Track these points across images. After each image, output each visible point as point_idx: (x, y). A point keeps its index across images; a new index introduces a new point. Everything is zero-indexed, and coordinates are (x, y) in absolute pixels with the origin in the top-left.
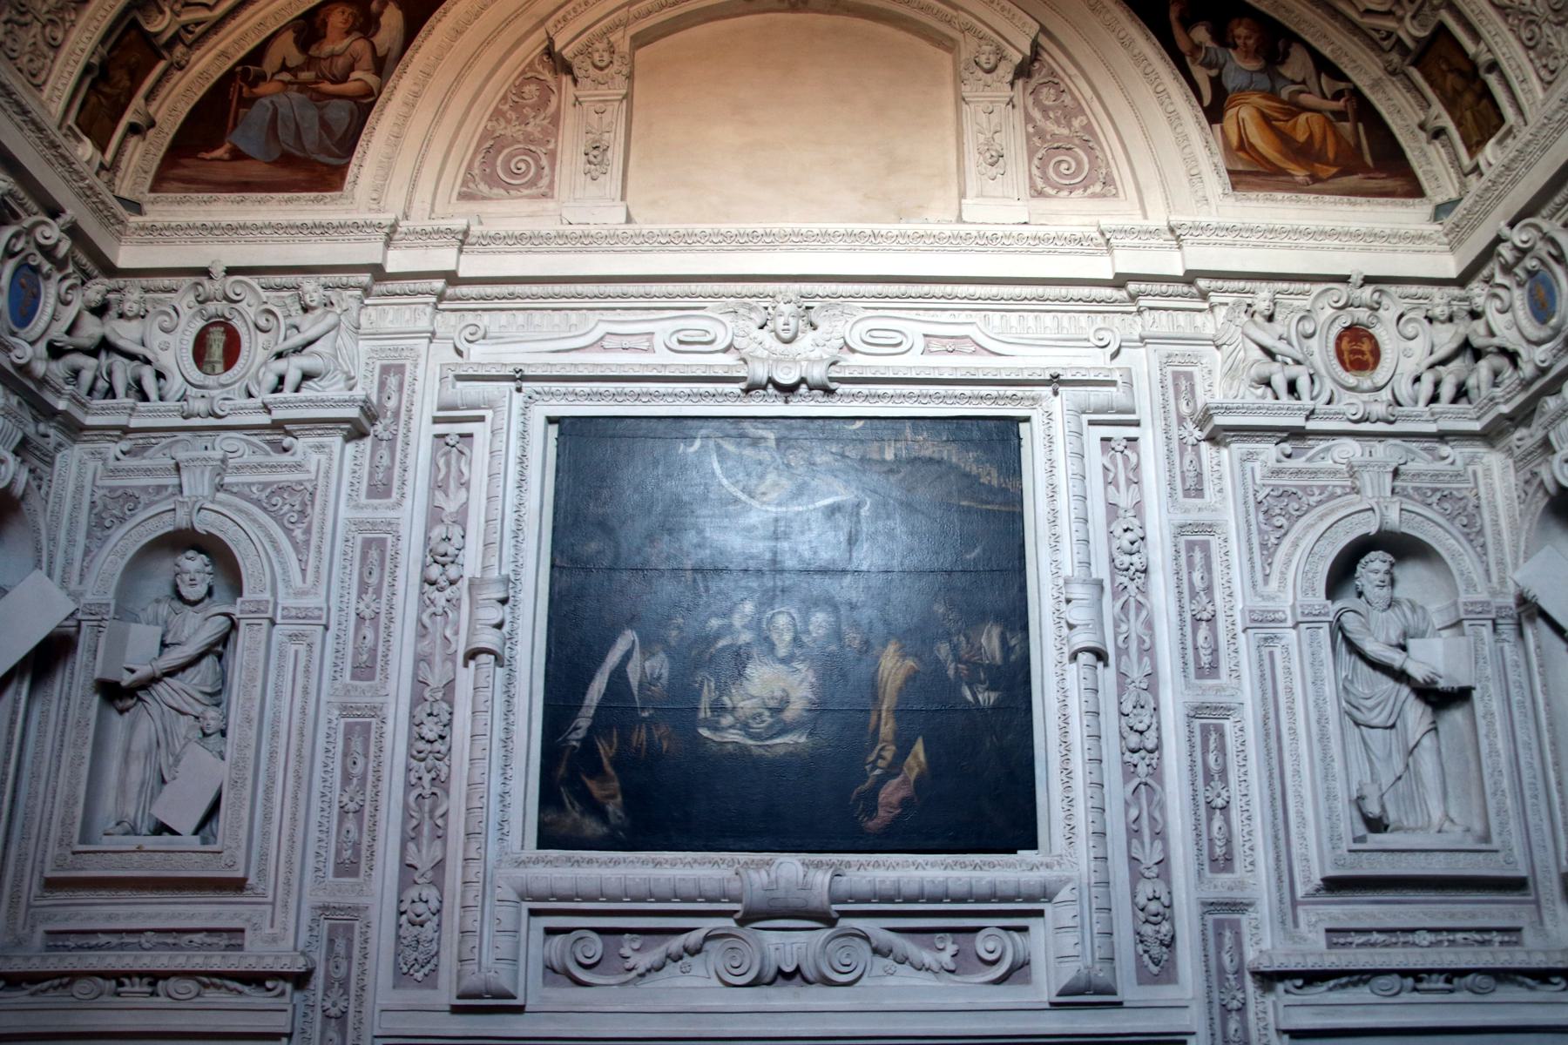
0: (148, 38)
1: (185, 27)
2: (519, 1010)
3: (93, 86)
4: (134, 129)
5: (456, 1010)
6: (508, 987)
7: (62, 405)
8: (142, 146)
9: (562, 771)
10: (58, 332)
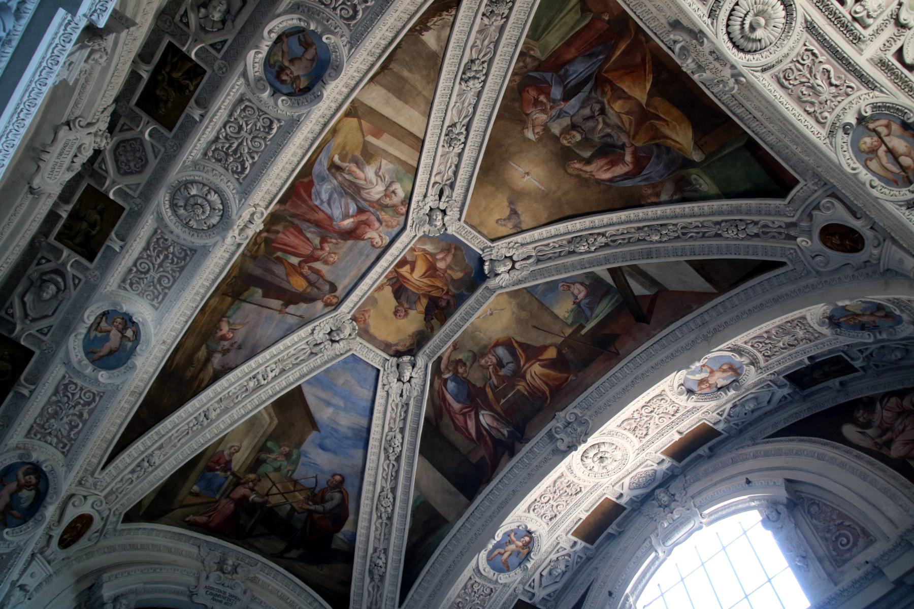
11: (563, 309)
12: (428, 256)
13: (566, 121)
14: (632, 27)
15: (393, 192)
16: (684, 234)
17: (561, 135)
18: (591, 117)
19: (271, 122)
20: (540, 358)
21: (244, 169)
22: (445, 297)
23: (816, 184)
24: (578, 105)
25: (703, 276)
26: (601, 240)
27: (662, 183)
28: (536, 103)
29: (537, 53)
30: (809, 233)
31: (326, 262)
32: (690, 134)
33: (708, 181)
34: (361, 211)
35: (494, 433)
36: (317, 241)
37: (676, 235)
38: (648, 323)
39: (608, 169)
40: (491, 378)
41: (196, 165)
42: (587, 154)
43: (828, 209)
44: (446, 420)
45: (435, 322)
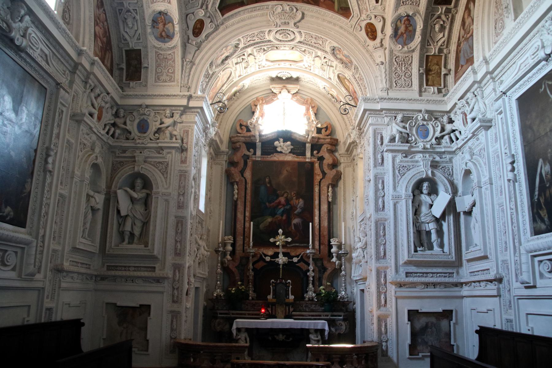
0: (434, 55)
1: (441, 46)
2: (534, 287)
3: (427, 75)
4: (446, 75)
5: (527, 287)
6: (528, 281)
7: (443, 150)
8: (451, 76)
9: (535, 210)
10: (438, 134)
14: (312, 2)
23: (220, 22)
30: (204, 16)
43: (211, 26)
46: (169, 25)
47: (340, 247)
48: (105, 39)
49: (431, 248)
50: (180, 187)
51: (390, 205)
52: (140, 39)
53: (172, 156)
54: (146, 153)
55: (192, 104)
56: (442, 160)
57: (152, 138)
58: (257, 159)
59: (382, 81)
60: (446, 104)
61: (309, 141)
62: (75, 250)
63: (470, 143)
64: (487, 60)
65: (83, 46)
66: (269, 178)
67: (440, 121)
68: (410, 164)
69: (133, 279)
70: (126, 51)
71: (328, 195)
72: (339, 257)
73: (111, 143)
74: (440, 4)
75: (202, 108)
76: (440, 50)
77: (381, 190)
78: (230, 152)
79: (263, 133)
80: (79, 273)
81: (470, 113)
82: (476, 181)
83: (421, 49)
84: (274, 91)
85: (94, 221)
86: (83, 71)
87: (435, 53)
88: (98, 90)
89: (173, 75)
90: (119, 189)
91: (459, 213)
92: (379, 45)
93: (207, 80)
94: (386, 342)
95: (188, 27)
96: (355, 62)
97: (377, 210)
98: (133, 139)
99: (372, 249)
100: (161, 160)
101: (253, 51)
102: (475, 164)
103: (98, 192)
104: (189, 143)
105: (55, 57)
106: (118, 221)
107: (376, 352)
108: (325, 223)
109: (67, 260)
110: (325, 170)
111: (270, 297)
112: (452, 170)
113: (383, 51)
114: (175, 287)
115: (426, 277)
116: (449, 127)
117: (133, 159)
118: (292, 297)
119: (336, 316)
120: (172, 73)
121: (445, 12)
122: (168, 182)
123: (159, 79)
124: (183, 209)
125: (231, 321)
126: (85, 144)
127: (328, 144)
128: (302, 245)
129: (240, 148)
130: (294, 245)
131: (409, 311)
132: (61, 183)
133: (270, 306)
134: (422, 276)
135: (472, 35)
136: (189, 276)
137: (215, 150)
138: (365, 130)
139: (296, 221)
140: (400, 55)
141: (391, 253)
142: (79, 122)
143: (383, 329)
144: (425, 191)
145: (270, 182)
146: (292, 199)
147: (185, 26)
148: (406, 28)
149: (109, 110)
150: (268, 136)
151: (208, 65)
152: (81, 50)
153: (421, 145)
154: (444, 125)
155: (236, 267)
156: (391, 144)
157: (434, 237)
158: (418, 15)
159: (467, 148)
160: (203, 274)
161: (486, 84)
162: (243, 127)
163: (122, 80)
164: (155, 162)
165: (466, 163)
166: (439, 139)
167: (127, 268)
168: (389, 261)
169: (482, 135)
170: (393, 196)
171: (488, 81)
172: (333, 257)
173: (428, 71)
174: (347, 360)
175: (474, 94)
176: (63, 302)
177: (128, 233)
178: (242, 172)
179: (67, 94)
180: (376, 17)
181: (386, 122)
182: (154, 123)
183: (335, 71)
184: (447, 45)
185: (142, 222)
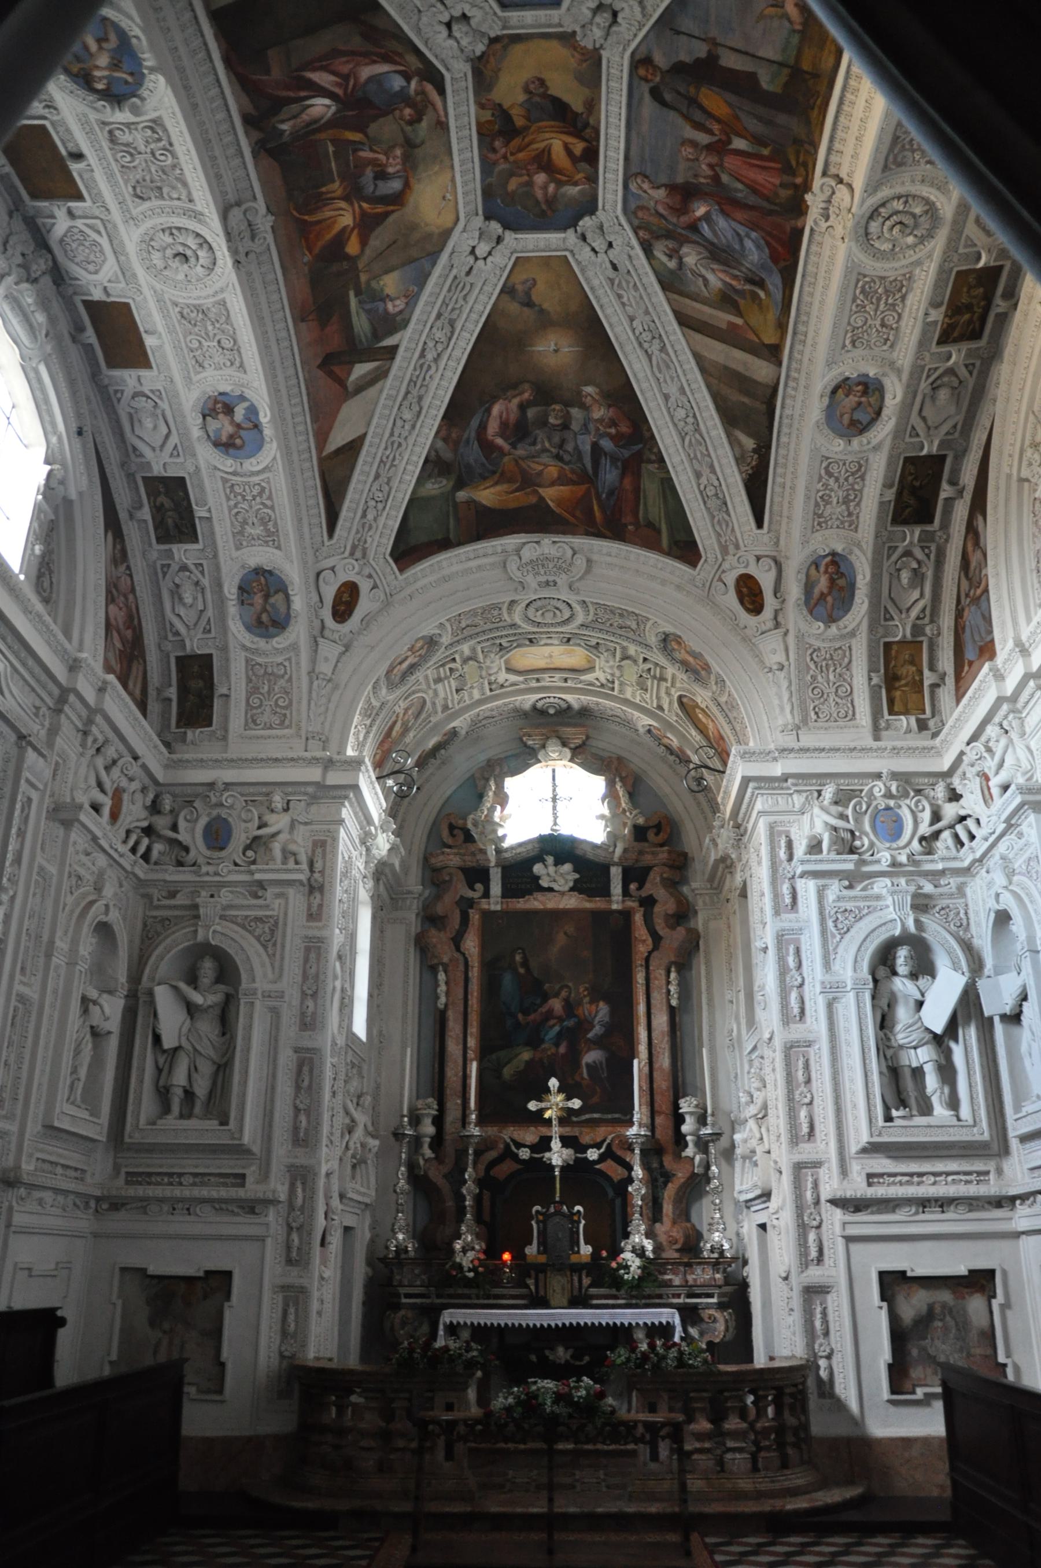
1: (918, 618)
4: (934, 686)
7: (940, 866)
10: (925, 829)
11: (390, 283)
12: (564, 178)
13: (575, 426)
14: (608, 533)
15: (670, 257)
16: (393, 443)
17: (568, 412)
18: (561, 446)
19: (854, 346)
20: (356, 232)
21: (863, 291)
22: (504, 150)
24: (581, 447)
25: (344, 446)
26: (430, 356)
27: (455, 451)
28: (613, 423)
29: (652, 467)
31: (694, 144)
32: (485, 502)
33: (434, 492)
34: (694, 227)
35: (294, 108)
36: (725, 178)
37: (396, 434)
38: (319, 367)
39: (501, 417)
40: (372, 150)
41: (918, 263)
42: (531, 413)
44: (357, 42)
45: (487, 115)
46: (277, 597)
47: (702, 1120)
48: (129, 634)
49: (926, 1109)
50: (305, 976)
51: (816, 1006)
52: (209, 631)
53: (287, 903)
54: (225, 896)
55: (334, 778)
56: (940, 890)
57: (238, 861)
58: (493, 908)
59: (782, 709)
60: (939, 754)
61: (616, 859)
62: (51, 1130)
63: (1002, 847)
64: (1023, 645)
65: (80, 650)
66: (524, 953)
67: (927, 798)
68: (861, 904)
69: (189, 1206)
70: (178, 658)
71: (669, 991)
72: (703, 1145)
73: (141, 875)
74: (905, 522)
75: (356, 788)
76: (917, 630)
77: (794, 972)
78: (427, 893)
79: (506, 845)
80: (57, 1191)
81: (997, 773)
82: (1022, 936)
83: (872, 629)
84: (530, 743)
85: (97, 1062)
86: (78, 705)
87: (904, 636)
88: (113, 749)
89: (288, 712)
90: (159, 984)
91: (991, 1019)
92: (770, 624)
93: (368, 722)
94: (829, 1357)
95: (321, 601)
96: (715, 667)
97: (786, 1019)
98: (194, 865)
99: (778, 1119)
100: (260, 913)
101: (473, 650)
102: (1015, 894)
103: (110, 992)
104: (327, 872)
105: (16, 676)
106: (156, 1062)
107: (804, 1383)
108: (664, 1061)
109: (31, 1156)
110: (658, 928)
111: (531, 1250)
112: (966, 913)
113: (780, 639)
114: (294, 1225)
115: (919, 1184)
116: (950, 811)
117: (194, 913)
118: (586, 1250)
119: (699, 1296)
120: (285, 708)
121: (919, 541)
122: (277, 964)
123: (254, 722)
124: (313, 1030)
125: (432, 1314)
126: (79, 878)
127: (664, 865)
128: (610, 1116)
129: (450, 881)
130: (587, 1116)
131: (882, 1275)
132: (23, 969)
133: (533, 1273)
134: (908, 1183)
135: (986, 591)
136: (328, 1197)
137: (389, 888)
138: (750, 826)
139: (592, 1056)
140: (822, 645)
141: (826, 1127)
142: (67, 824)
143: (818, 1324)
144: (902, 968)
145: (525, 963)
146: (580, 1003)
147: (316, 598)
148: (832, 581)
149: (139, 796)
150: (519, 850)
151: (370, 687)
152: (75, 660)
153: (885, 857)
154: (939, 806)
155: (445, 1176)
156: (813, 857)
157: (932, 1081)
158: (856, 551)
159: (997, 857)
160: (364, 1194)
161: (1027, 703)
162: (456, 832)
163: (169, 726)
164: (247, 917)
165: (998, 895)
166: (929, 841)
167: (174, 1178)
168: (822, 1146)
169: (1030, 825)
170: (823, 983)
171: (1032, 695)
172: (686, 1146)
173: (891, 680)
174: (729, 1404)
175: (1002, 727)
176: (16, 1264)
177: (179, 1092)
178: (457, 941)
179: (41, 760)
180: (758, 558)
181: (797, 806)
182: (243, 825)
183: (673, 691)
184: (932, 615)
185: (214, 1063)
